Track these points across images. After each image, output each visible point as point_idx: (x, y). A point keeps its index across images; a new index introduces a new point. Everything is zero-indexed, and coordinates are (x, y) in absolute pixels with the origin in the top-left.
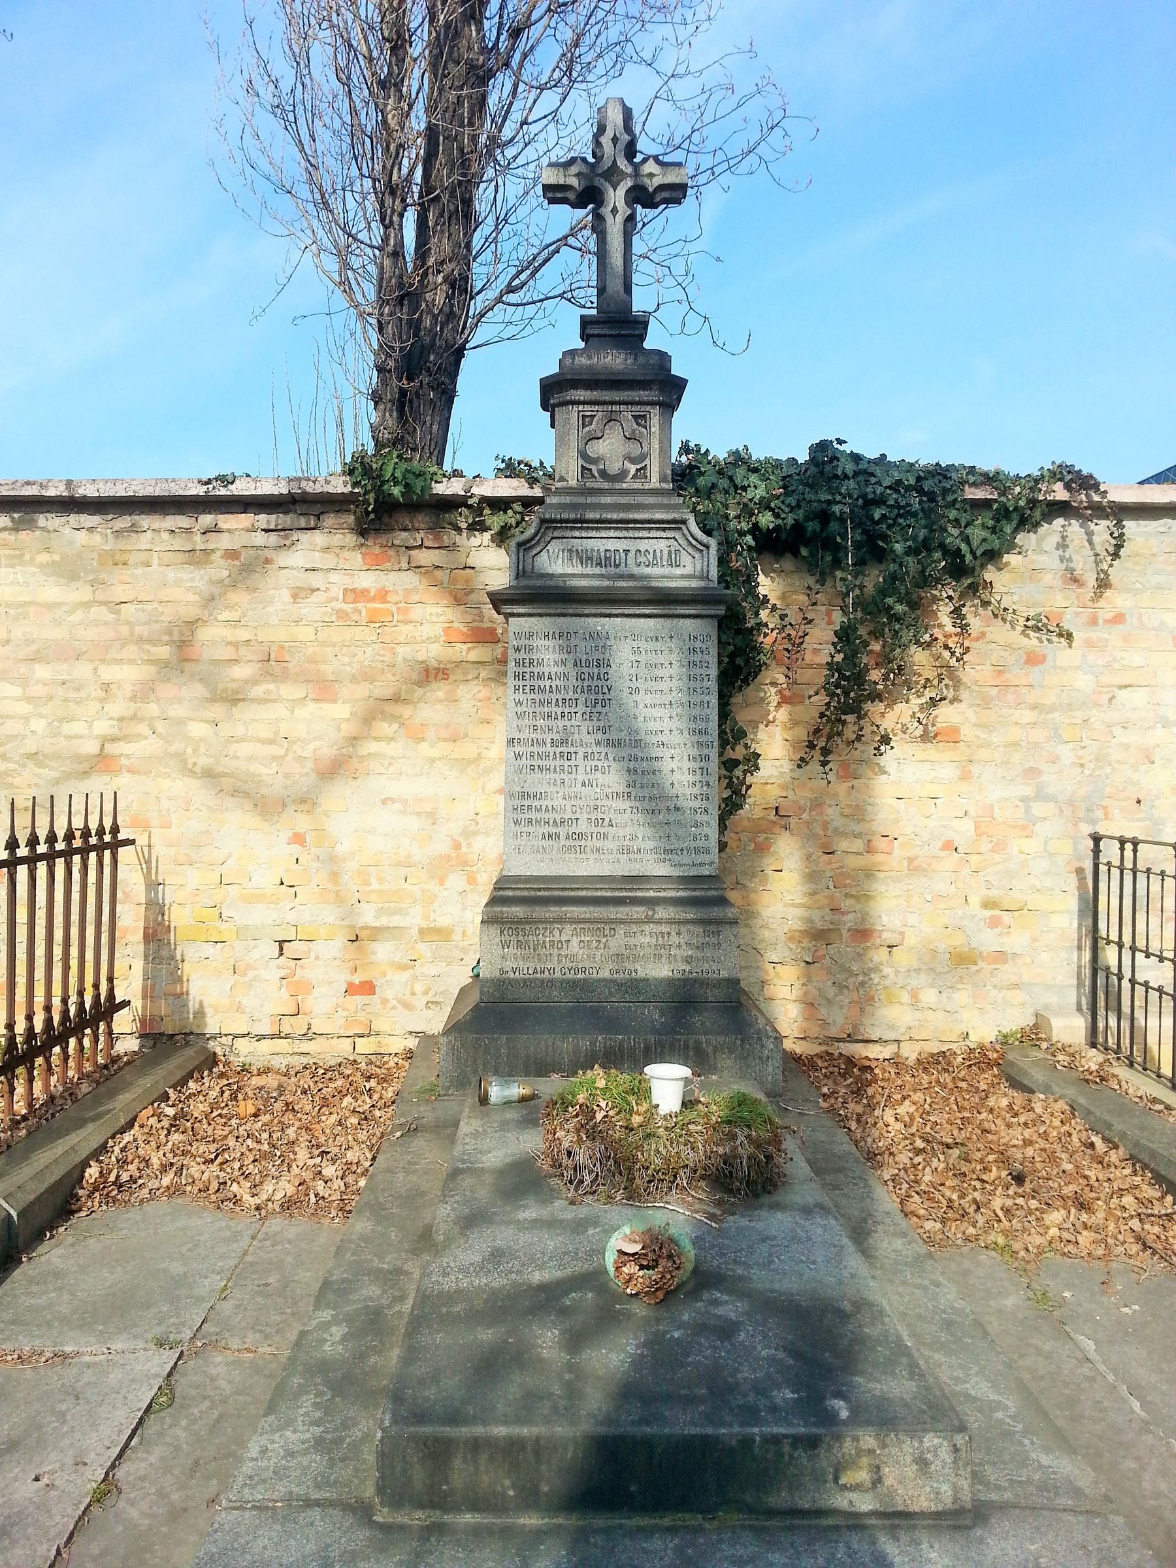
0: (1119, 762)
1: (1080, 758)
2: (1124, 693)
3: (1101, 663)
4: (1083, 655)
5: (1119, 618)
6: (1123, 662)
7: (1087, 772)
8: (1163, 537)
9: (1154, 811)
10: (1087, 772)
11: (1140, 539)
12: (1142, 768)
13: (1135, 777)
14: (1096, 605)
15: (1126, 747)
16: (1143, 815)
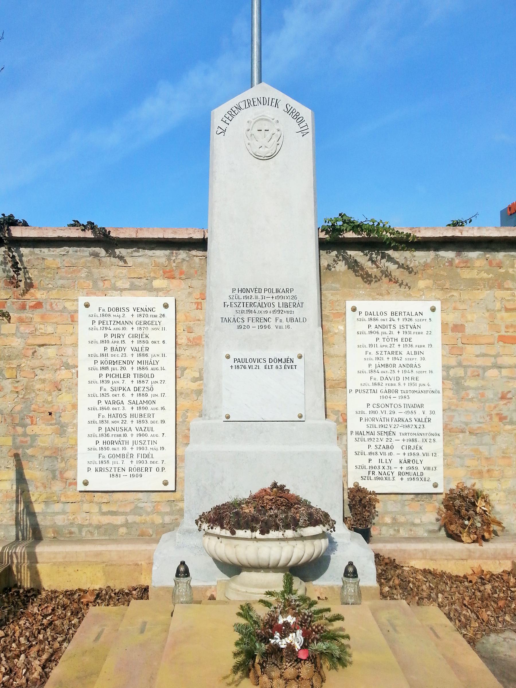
0: (39, 390)
1: (16, 388)
2: (42, 348)
3: (28, 332)
4: (17, 327)
5: (39, 305)
6: (41, 331)
7: (21, 396)
8: (65, 257)
9: (61, 419)
10: (21, 396)
11: (50, 259)
12: (54, 393)
13: (50, 399)
14: (24, 298)
15: (43, 381)
16: (54, 422)
